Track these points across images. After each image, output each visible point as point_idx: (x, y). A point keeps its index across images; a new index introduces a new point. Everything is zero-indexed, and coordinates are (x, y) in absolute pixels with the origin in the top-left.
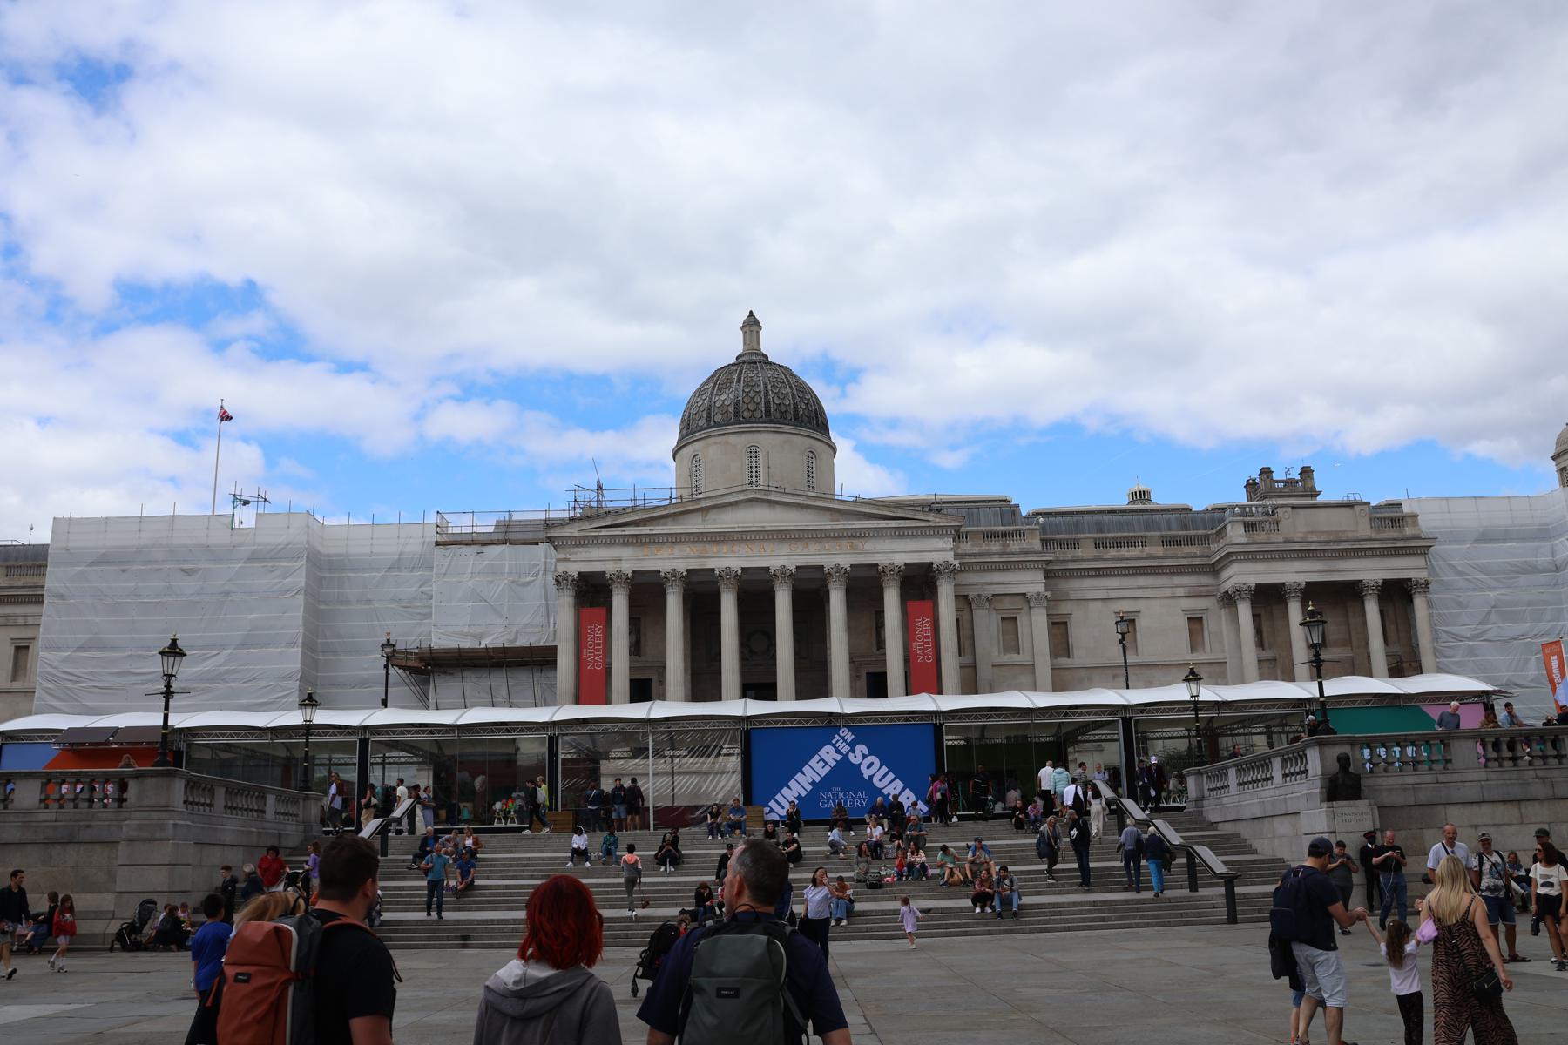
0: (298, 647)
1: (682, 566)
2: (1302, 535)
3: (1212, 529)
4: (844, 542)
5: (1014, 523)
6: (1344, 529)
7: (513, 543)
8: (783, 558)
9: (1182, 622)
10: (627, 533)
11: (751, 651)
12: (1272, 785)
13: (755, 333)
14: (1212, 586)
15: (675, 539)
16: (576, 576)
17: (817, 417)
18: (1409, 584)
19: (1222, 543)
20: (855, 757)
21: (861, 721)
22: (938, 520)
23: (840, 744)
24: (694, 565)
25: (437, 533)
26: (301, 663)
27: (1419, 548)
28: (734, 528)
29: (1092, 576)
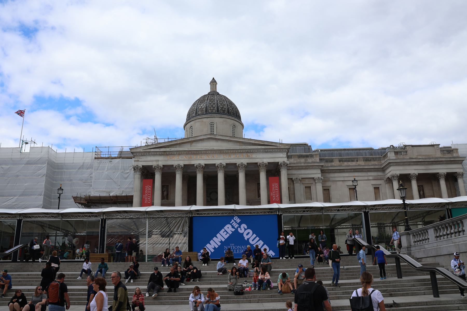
0: (42, 196)
1: (182, 163)
2: (416, 156)
3: (381, 156)
4: (245, 155)
5: (309, 152)
6: (431, 154)
7: (123, 158)
8: (221, 160)
9: (372, 189)
10: (161, 150)
11: (211, 199)
12: (464, 234)
13: (214, 85)
14: (382, 176)
15: (179, 153)
16: (141, 167)
17: (236, 113)
18: (456, 174)
19: (386, 160)
20: (241, 230)
21: (244, 213)
22: (281, 146)
23: (234, 224)
24: (187, 163)
25: (95, 154)
26: (43, 202)
27: (459, 161)
28: (202, 148)
29: (338, 172)
